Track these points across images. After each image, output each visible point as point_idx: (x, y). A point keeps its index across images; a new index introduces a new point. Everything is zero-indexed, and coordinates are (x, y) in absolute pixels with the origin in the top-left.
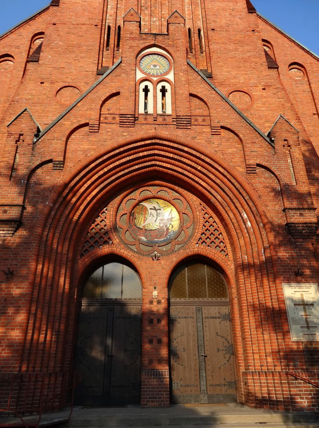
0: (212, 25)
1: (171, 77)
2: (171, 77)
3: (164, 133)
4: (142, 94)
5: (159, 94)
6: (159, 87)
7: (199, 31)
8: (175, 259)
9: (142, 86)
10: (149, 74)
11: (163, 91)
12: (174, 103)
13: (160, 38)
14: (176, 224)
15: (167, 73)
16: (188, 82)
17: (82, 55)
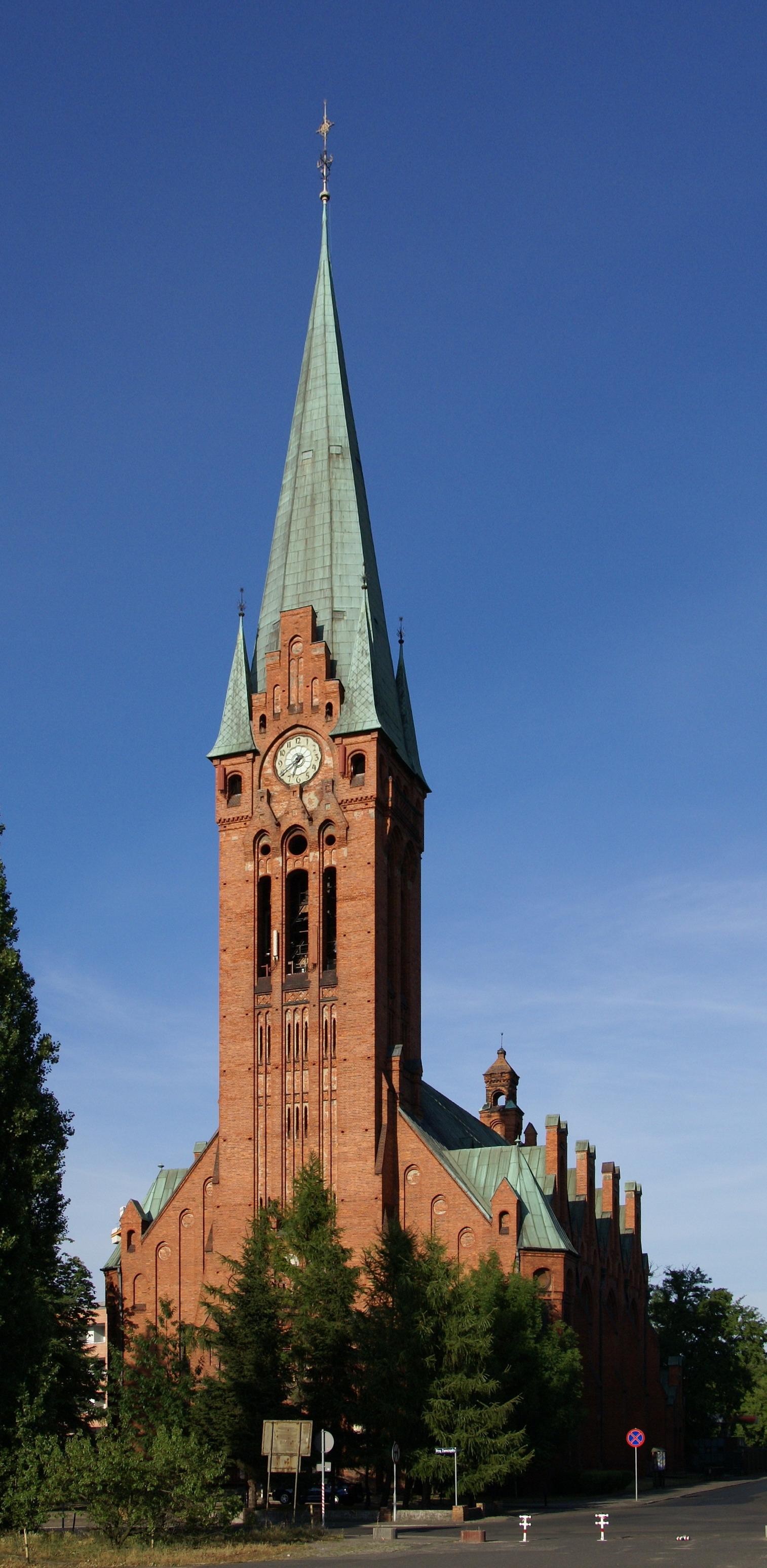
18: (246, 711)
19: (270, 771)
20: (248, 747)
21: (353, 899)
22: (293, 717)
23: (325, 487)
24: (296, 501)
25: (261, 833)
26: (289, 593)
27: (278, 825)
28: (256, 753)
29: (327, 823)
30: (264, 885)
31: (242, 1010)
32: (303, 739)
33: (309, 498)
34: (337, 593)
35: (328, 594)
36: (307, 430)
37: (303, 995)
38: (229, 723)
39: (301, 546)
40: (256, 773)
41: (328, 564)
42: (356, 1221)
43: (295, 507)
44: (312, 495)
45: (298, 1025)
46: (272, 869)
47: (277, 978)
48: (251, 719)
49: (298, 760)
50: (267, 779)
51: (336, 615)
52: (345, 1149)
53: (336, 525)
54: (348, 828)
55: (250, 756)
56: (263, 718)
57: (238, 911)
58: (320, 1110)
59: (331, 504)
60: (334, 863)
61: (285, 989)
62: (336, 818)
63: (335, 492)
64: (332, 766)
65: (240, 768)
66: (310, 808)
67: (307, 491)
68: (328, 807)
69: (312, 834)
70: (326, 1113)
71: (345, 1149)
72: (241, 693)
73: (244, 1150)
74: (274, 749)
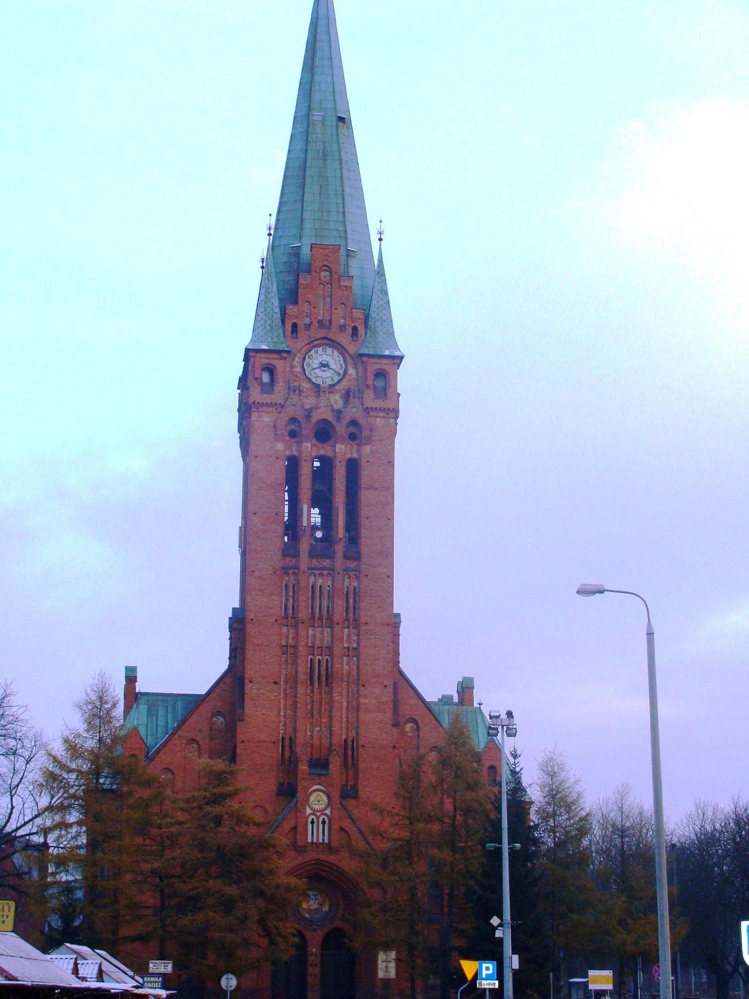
0: (362, 742)
1: (328, 812)
2: (328, 812)
3: (323, 857)
4: (310, 826)
5: (321, 826)
6: (321, 820)
7: (353, 741)
8: (326, 930)
9: (310, 819)
10: (314, 810)
11: (324, 822)
12: (329, 835)
13: (323, 778)
14: (326, 908)
15: (326, 808)
16: (340, 819)
17: (266, 775)
18: (278, 316)
19: (299, 369)
20: (284, 347)
21: (375, 489)
22: (321, 331)
23: (335, 149)
24: (309, 152)
25: (293, 420)
26: (307, 225)
27: (308, 417)
28: (289, 352)
29: (354, 423)
30: (293, 464)
31: (271, 568)
32: (329, 350)
33: (321, 152)
34: (349, 236)
35: (342, 234)
36: (316, 97)
37: (326, 563)
38: (263, 322)
39: (316, 189)
40: (288, 369)
41: (341, 210)
42: (375, 765)
43: (309, 157)
44: (324, 151)
45: (321, 587)
46: (299, 451)
47: (304, 546)
48: (283, 322)
49: (324, 366)
50: (296, 376)
51: (349, 254)
52: (366, 701)
53: (345, 181)
54: (371, 431)
55: (285, 355)
56: (295, 326)
57: (269, 482)
58: (342, 664)
59: (341, 163)
60: (355, 456)
61: (311, 556)
62: (362, 421)
63: (343, 154)
64: (355, 376)
65: (274, 362)
66: (337, 407)
67: (319, 146)
68: (354, 410)
69: (341, 429)
70: (346, 667)
71: (366, 701)
72: (273, 300)
73: (269, 692)
74: (302, 352)
